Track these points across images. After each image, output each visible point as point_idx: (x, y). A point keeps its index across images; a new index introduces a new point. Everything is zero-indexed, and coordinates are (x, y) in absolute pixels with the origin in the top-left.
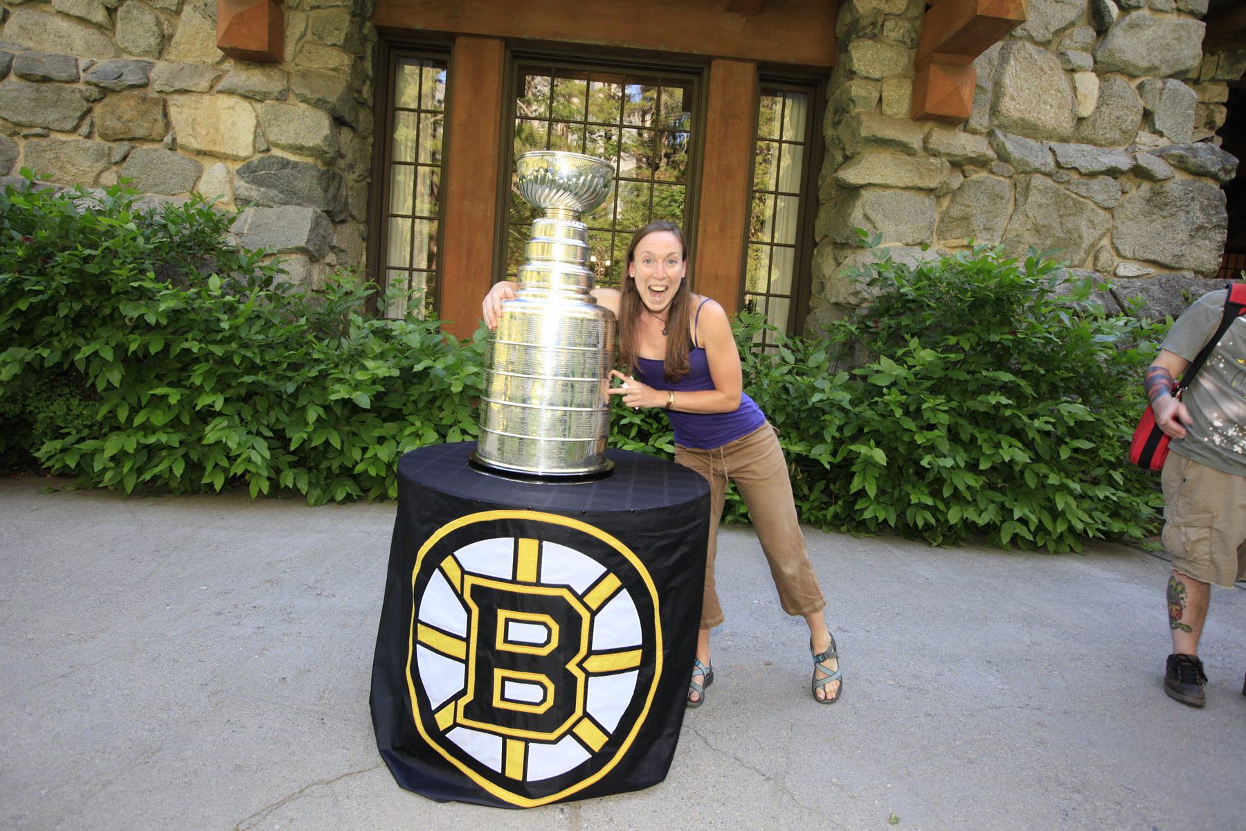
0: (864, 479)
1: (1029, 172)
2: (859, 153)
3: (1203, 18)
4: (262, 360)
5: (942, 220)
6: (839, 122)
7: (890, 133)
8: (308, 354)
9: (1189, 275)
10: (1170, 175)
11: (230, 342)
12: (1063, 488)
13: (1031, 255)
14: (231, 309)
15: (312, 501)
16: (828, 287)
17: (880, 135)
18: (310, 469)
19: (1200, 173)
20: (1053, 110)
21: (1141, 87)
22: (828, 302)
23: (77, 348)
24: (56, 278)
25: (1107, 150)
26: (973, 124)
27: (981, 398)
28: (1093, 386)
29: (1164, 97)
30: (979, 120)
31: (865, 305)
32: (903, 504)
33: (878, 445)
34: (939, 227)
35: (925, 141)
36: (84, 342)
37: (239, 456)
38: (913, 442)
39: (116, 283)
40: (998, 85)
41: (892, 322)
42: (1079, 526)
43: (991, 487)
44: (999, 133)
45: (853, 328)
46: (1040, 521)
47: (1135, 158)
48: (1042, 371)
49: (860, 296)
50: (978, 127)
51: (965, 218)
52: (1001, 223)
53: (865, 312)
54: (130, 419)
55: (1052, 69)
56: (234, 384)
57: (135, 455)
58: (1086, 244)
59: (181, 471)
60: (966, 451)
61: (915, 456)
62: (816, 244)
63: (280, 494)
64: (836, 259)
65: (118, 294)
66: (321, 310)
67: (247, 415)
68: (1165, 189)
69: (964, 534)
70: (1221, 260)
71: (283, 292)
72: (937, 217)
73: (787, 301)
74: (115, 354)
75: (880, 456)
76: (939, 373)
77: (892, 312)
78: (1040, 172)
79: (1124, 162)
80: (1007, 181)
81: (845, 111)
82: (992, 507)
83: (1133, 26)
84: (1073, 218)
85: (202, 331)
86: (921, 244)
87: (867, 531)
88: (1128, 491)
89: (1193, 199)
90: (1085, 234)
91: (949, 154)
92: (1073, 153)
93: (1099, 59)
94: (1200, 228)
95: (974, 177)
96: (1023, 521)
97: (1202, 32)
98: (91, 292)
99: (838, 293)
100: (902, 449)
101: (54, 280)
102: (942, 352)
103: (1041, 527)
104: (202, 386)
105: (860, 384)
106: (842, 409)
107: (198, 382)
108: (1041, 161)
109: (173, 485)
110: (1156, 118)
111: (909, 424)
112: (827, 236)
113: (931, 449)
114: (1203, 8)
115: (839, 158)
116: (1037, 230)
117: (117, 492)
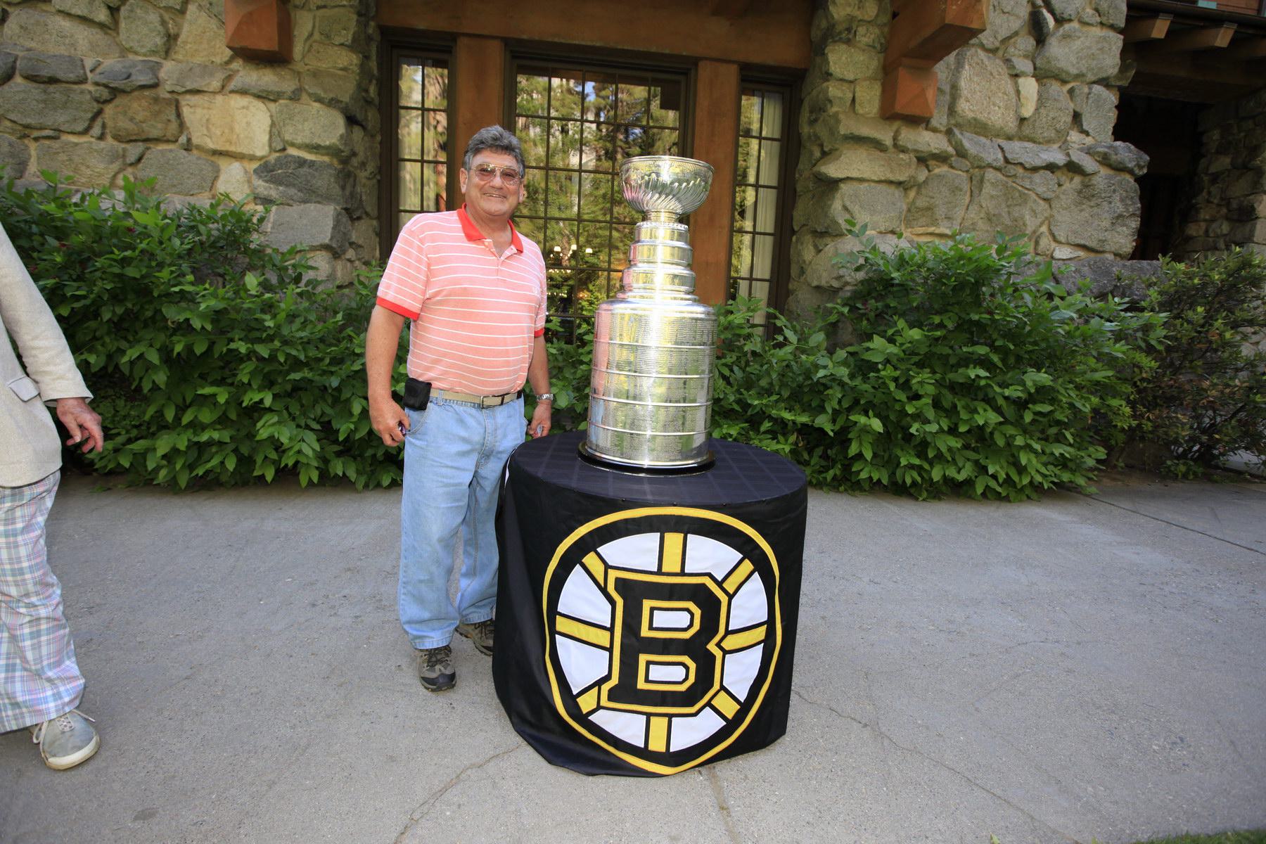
0: (861, 444)
1: (983, 167)
2: (836, 150)
3: (1121, 32)
4: (306, 357)
5: (909, 210)
6: (816, 120)
7: (865, 131)
8: (347, 348)
9: (1110, 257)
10: (1097, 170)
11: (272, 341)
12: (1028, 447)
13: (1000, 242)
14: (269, 307)
15: (360, 486)
16: (809, 271)
17: (857, 133)
18: (355, 458)
19: (1119, 168)
20: (1000, 112)
21: (1071, 91)
22: (809, 285)
23: (123, 352)
24: (99, 283)
25: (1045, 147)
26: (934, 123)
27: (961, 370)
28: (1049, 357)
29: (1090, 101)
30: (940, 119)
31: (848, 288)
32: (893, 464)
33: (876, 416)
34: (906, 217)
35: (895, 139)
36: (127, 345)
37: (292, 447)
38: (903, 413)
39: (158, 286)
40: (955, 87)
41: (880, 305)
42: (1039, 478)
43: (966, 447)
44: (956, 131)
45: (846, 310)
46: (1007, 474)
47: (1068, 155)
48: (1012, 347)
49: (843, 280)
50: (938, 126)
51: (929, 209)
52: (959, 213)
53: (849, 294)
54: (178, 419)
55: (999, 74)
56: (280, 381)
57: (186, 452)
58: (1029, 231)
59: (234, 466)
60: (946, 417)
61: (904, 423)
62: (793, 232)
63: (329, 482)
64: (816, 246)
65: (159, 296)
66: (354, 305)
67: (295, 409)
68: (1094, 182)
69: (944, 489)
70: (1134, 244)
71: (314, 288)
72: (905, 207)
73: (767, 284)
74: (161, 358)
75: (877, 425)
76: (923, 350)
77: (874, 294)
78: (992, 167)
79: (1060, 159)
80: (965, 174)
81: (822, 110)
82: (969, 466)
83: (1066, 37)
84: (1017, 208)
85: (243, 330)
86: (893, 232)
87: (862, 490)
88: (1070, 445)
89: (1114, 191)
90: (1028, 222)
91: (916, 151)
92: (1017, 150)
93: (1038, 65)
94: (1120, 216)
95: (937, 171)
96: (994, 477)
97: (1120, 44)
98: (131, 296)
99: (820, 278)
100: (892, 417)
101: (95, 285)
102: (928, 331)
103: (1009, 481)
104: (249, 384)
105: (851, 360)
106: (842, 384)
107: (246, 381)
108: (993, 157)
109: (224, 478)
110: (1084, 119)
111: (902, 396)
112: (804, 225)
113: (918, 416)
114: (1121, 23)
115: (817, 154)
116: (989, 218)
117: (172, 488)
